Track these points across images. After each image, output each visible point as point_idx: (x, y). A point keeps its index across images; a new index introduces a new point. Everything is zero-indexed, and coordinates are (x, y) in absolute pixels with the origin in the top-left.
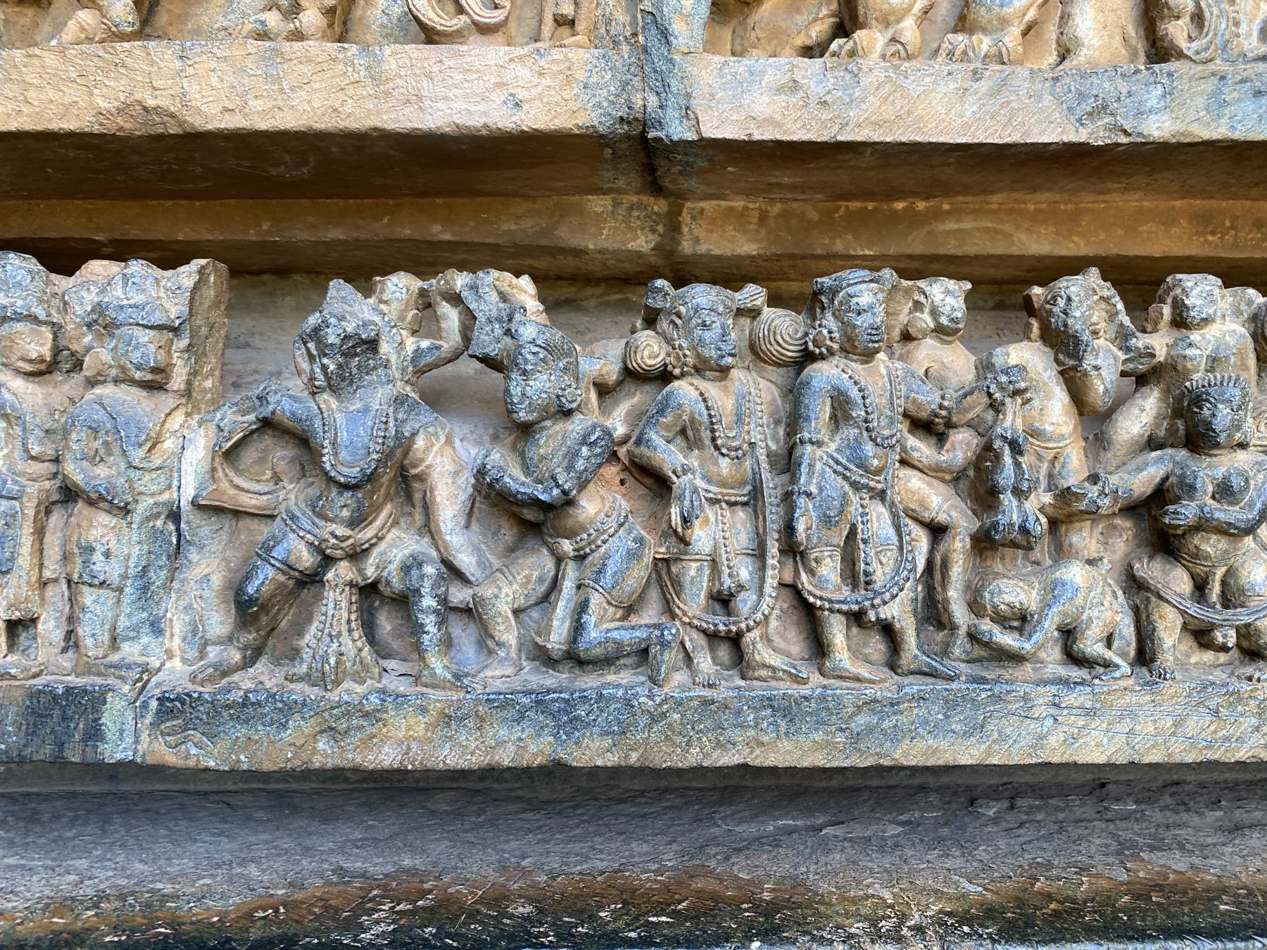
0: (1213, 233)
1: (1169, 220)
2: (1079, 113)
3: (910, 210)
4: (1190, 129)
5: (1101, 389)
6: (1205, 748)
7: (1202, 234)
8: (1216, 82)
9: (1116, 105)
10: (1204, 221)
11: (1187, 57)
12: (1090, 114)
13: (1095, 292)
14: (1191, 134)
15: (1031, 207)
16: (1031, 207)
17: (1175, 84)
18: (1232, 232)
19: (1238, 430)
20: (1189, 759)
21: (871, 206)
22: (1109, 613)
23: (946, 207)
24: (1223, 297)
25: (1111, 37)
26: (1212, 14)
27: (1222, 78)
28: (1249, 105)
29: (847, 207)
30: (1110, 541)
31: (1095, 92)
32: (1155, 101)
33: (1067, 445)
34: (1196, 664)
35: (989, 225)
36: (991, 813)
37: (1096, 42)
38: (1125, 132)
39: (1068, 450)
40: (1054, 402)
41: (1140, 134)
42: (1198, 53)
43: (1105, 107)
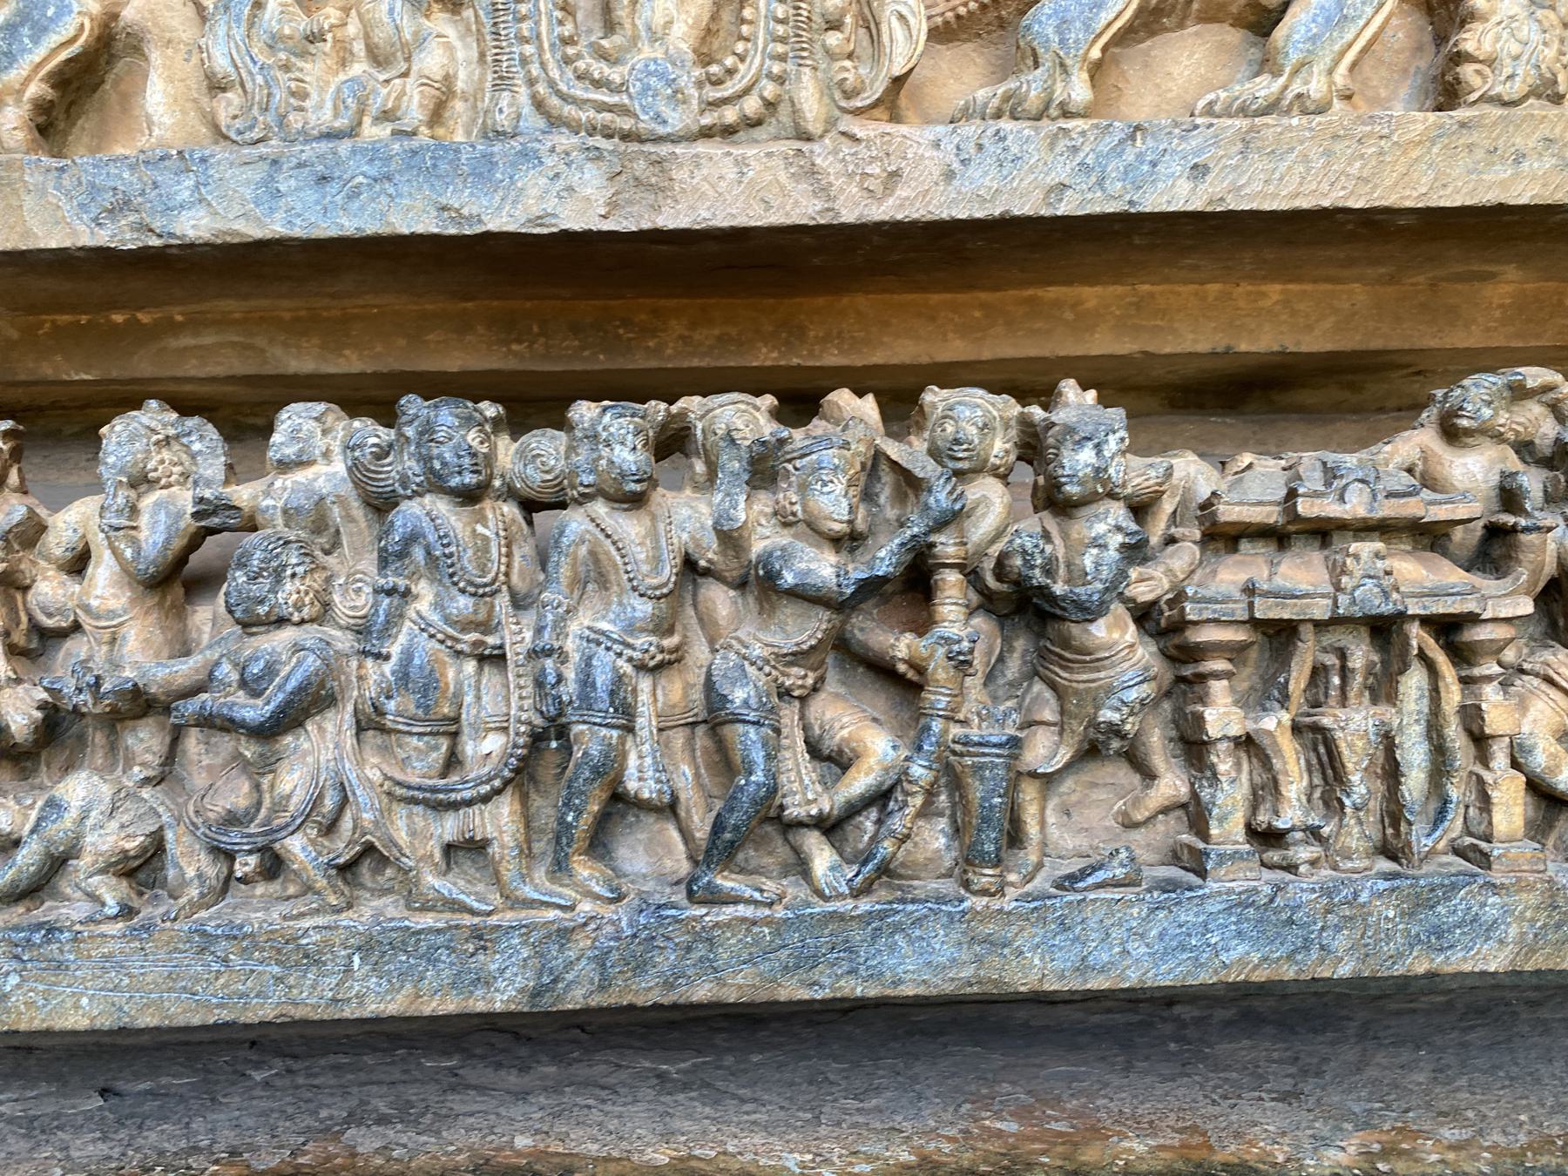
0: (519, 342)
1: (463, 326)
2: (94, 211)
3: (133, 323)
4: (236, 227)
5: (128, 553)
6: (218, 1006)
7: (507, 343)
8: (266, 167)
9: (140, 199)
10: (508, 328)
11: (226, 138)
12: (111, 211)
13: (153, 431)
14: (237, 233)
15: (287, 315)
16: (287, 315)
17: (211, 172)
18: (542, 340)
19: (261, 602)
20: (196, 1021)
21: (84, 319)
22: (111, 839)
23: (179, 318)
24: (325, 432)
25: (184, 112)
26: (253, 80)
27: (275, 162)
28: (310, 195)
29: (53, 322)
30: (213, 740)
31: (112, 184)
32: (187, 193)
33: (121, 624)
34: (262, 896)
35: (236, 339)
36: (258, 1078)
37: (168, 121)
38: (151, 230)
39: (124, 630)
40: (100, 570)
41: (171, 235)
42: (240, 133)
43: (127, 202)
